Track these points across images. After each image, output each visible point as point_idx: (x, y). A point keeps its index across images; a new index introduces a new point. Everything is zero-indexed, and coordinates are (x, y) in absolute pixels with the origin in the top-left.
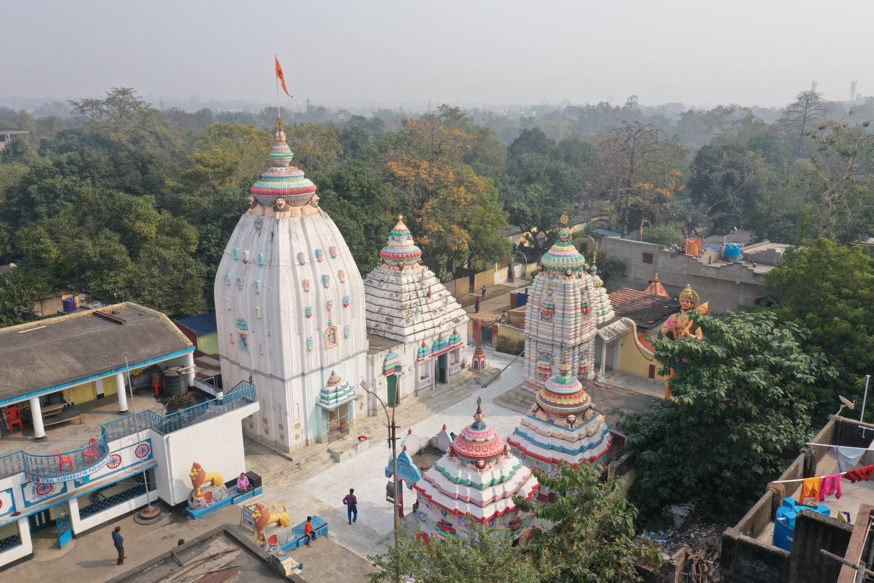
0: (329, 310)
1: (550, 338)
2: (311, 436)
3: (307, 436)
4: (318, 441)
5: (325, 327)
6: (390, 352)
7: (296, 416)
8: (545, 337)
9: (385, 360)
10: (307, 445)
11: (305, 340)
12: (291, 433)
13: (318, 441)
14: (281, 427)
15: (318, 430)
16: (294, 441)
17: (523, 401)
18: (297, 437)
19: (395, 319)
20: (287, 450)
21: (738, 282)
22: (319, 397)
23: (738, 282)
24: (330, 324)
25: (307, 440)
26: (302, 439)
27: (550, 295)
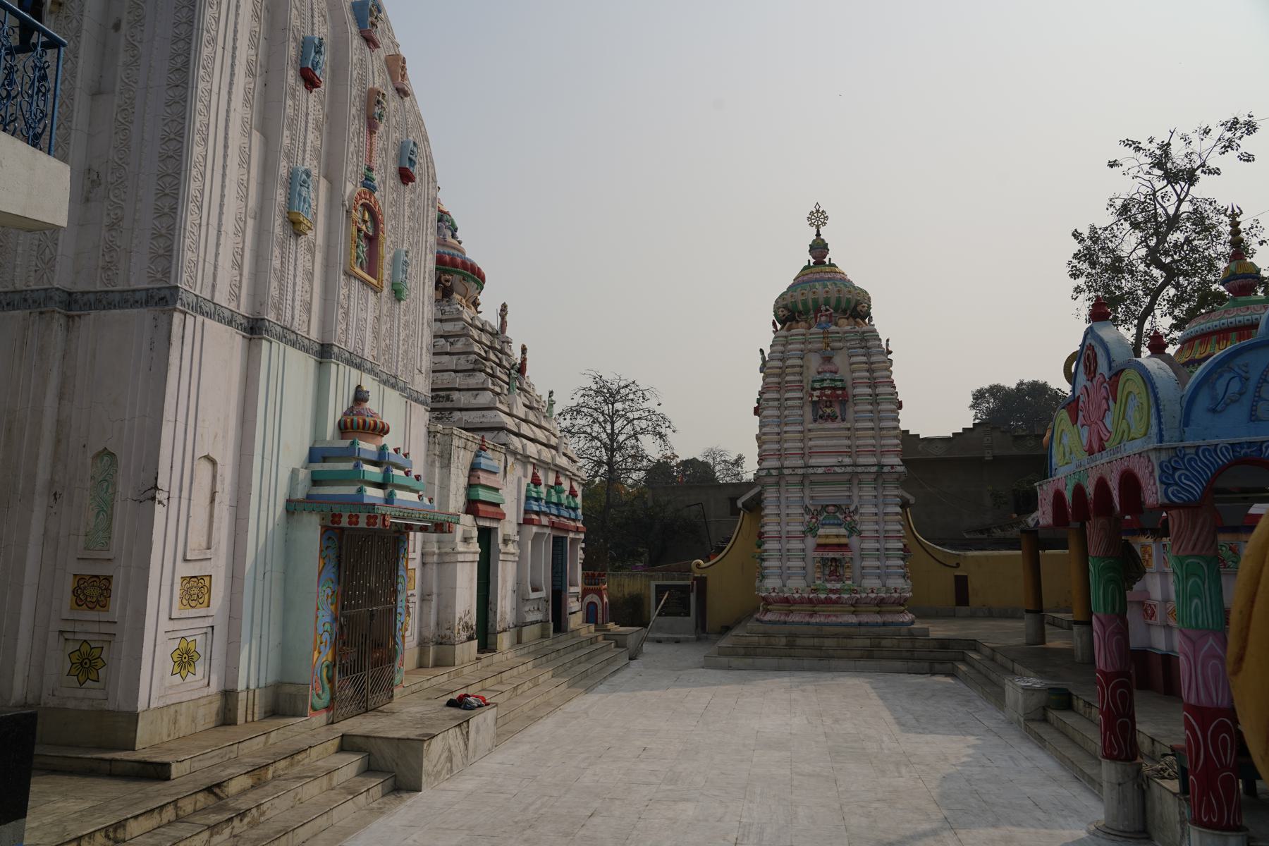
0: (372, 128)
1: (847, 460)
2: (250, 675)
3: (231, 668)
4: (282, 704)
5: (350, 188)
6: (482, 448)
7: (197, 539)
8: (831, 461)
9: (474, 468)
10: (226, 717)
11: (283, 171)
12: (164, 623)
13: (282, 704)
14: (93, 591)
15: (285, 650)
16: (166, 691)
17: (791, 645)
18: (185, 660)
19: (455, 395)
20: (124, 723)
21: (988, 457)
22: (303, 475)
23: (988, 457)
24: (368, 184)
25: (228, 695)
26: (200, 687)
27: (828, 359)
